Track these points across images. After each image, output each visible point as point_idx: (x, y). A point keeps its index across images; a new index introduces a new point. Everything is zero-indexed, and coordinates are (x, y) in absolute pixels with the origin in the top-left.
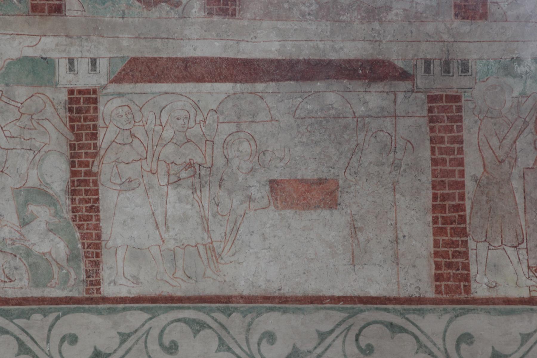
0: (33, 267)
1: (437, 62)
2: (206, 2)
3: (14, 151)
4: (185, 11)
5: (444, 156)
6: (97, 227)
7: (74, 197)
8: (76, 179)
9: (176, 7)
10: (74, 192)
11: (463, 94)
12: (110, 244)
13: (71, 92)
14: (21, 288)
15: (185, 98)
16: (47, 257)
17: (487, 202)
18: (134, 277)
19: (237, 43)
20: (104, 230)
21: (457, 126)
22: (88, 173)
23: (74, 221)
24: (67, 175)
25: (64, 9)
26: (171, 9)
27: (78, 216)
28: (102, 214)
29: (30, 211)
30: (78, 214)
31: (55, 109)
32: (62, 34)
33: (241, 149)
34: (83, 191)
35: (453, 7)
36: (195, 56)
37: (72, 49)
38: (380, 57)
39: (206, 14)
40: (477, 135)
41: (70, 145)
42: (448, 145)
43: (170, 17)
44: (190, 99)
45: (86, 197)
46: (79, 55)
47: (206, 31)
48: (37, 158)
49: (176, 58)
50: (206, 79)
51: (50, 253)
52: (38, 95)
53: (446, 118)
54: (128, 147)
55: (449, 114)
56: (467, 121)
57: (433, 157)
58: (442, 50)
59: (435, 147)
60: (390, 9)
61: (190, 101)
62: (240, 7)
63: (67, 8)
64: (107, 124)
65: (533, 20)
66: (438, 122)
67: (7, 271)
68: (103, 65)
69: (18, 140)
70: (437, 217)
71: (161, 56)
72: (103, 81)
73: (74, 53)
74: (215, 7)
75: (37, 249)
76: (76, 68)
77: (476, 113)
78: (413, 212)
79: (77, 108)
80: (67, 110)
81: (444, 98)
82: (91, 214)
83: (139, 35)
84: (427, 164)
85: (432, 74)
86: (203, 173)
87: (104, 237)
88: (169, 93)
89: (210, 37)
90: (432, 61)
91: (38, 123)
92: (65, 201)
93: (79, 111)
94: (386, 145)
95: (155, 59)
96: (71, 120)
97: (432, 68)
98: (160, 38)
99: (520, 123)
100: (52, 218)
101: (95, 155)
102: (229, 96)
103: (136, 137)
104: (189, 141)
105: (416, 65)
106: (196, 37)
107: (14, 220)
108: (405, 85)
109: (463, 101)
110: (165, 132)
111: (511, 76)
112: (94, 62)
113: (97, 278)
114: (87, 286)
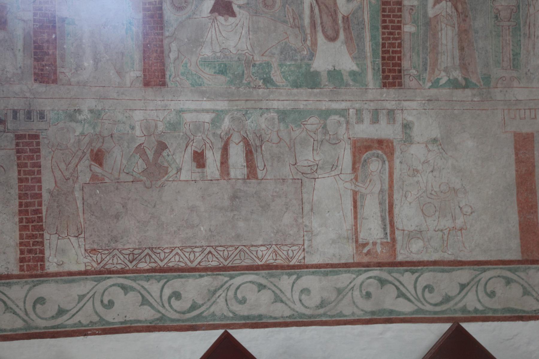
1: (22, 112)
5: (27, 176)
11: (41, 134)
17: (58, 207)
21: (37, 155)
35: (33, 75)
40: (50, 162)
42: (30, 169)
53: (28, 150)
55: (30, 148)
56: (43, 152)
57: (20, 177)
58: (25, 104)
59: (21, 170)
65: (89, 85)
66: (22, 153)
70: (22, 219)
77: (50, 146)
78: (4, 216)
81: (27, 136)
84: (14, 182)
85: (18, 120)
90: (18, 111)
97: (18, 116)
99: (80, 153)
105: (6, 114)
109: (41, 139)
111: (74, 121)
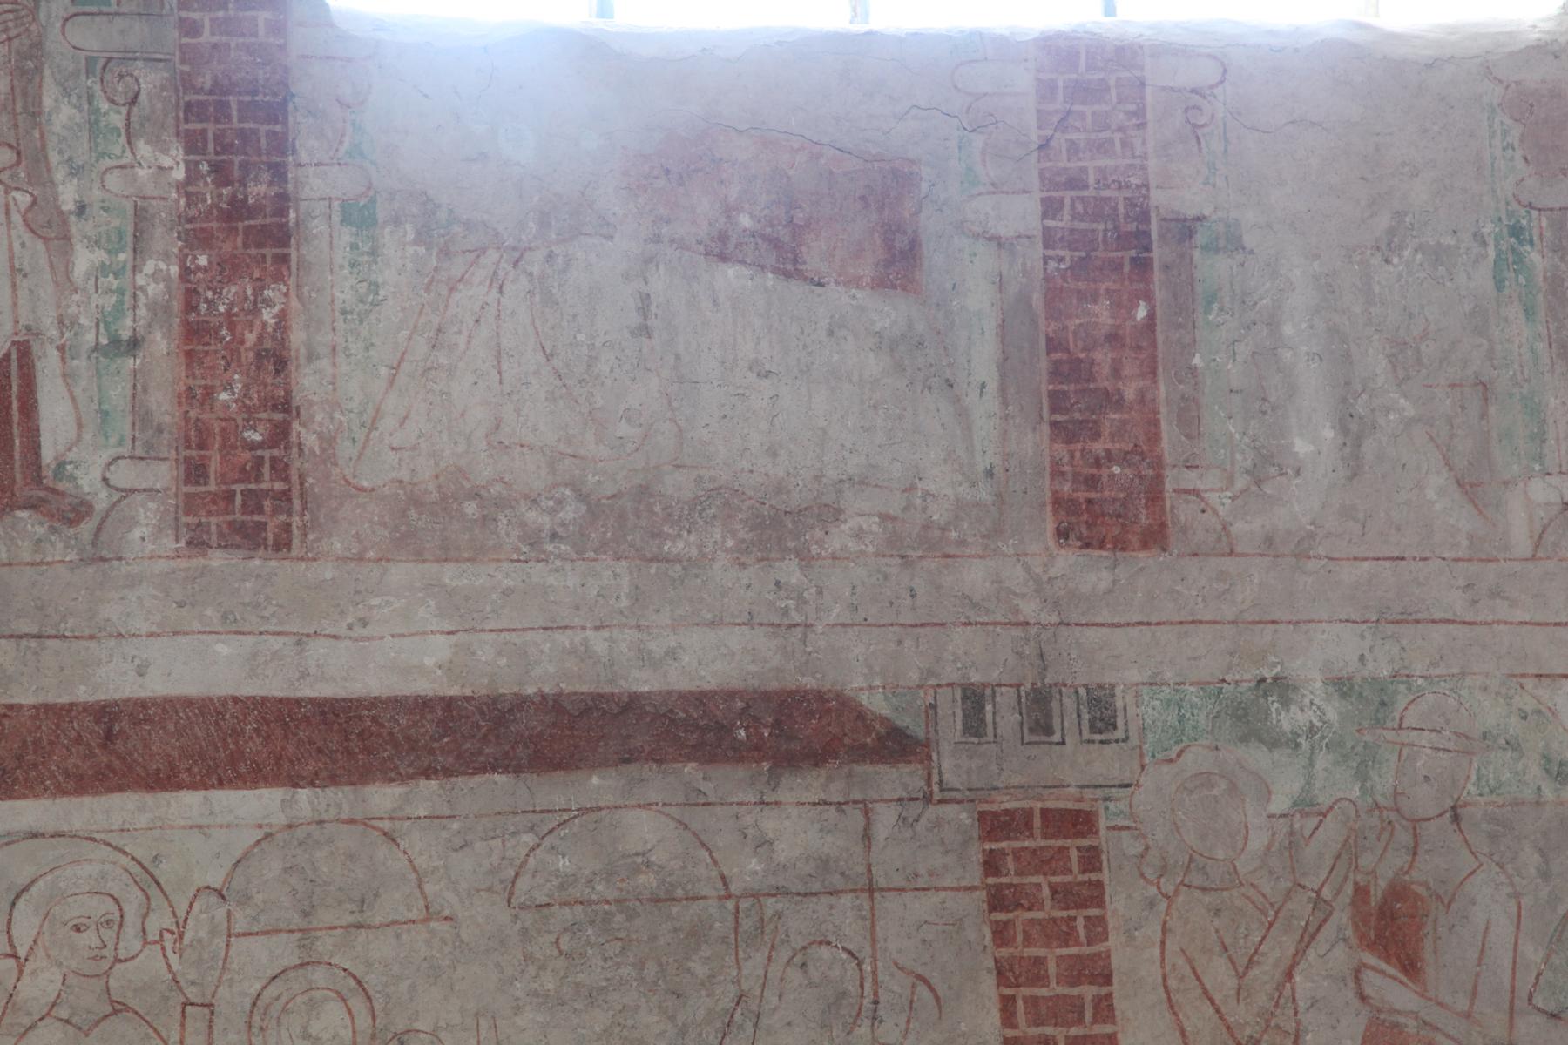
1: (1006, 697)
2: (181, 505)
4: (104, 537)
5: (1049, 1030)
9: (72, 523)
11: (1101, 805)
15: (105, 851)
19: (298, 643)
21: (1087, 918)
26: (53, 530)
33: (315, 1028)
35: (1049, 508)
36: (143, 694)
38: (809, 682)
39: (182, 544)
40: (1157, 951)
42: (1060, 990)
43: (49, 559)
44: (125, 853)
47: (181, 605)
49: (72, 704)
50: (184, 776)
53: (1046, 892)
55: (1057, 879)
56: (1119, 904)
57: (1010, 1033)
58: (1020, 655)
59: (1013, 998)
60: (837, 514)
61: (125, 860)
62: (307, 517)
65: (1321, 551)
66: (1019, 906)
71: (15, 701)
74: (213, 520)
77: (1150, 873)
81: (1037, 822)
85: (990, 738)
88: (43, 835)
89: (197, 626)
90: (988, 692)
94: (844, 994)
97: (989, 717)
98: (11, 636)
99: (1300, 906)
102: (268, 836)
104: (118, 1008)
105: (933, 707)
106: (145, 628)
108: (895, 779)
109: (1102, 832)
110: (26, 978)
111: (1261, 740)
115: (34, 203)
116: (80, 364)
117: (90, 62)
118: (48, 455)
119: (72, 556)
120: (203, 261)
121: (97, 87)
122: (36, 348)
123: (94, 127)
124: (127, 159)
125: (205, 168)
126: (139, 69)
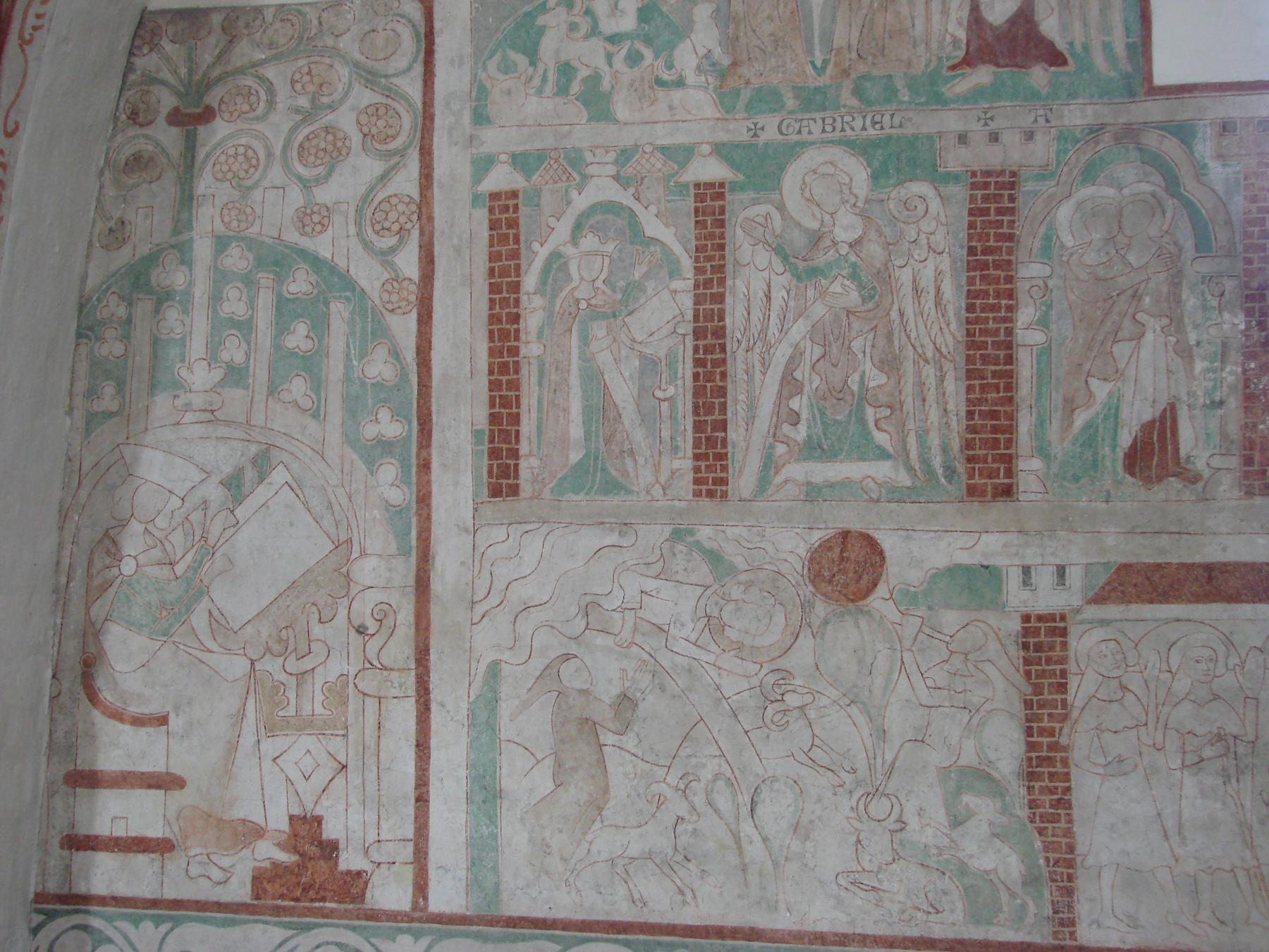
0: (970, 893)
3: (941, 709)
6: (1068, 833)
7: (1031, 784)
8: (1034, 755)
10: (1032, 776)
12: (1090, 861)
13: (1026, 618)
14: (953, 924)
15: (1208, 629)
16: (992, 877)
18: (1129, 916)
20: (1079, 839)
22: (1053, 747)
23: (1031, 822)
24: (1019, 749)
25: (1015, 490)
27: (1037, 814)
28: (1076, 813)
29: (964, 803)
30: (1038, 811)
31: (1002, 645)
32: (1013, 529)
34: (1046, 776)
37: (1028, 551)
39: (1242, 493)
41: (1026, 702)
45: (1050, 784)
46: (1039, 560)
47: (1242, 521)
48: (975, 721)
50: (1243, 597)
51: (995, 870)
52: (975, 623)
54: (1115, 706)
63: (1021, 489)
64: (1083, 669)
67: (930, 895)
68: (1075, 576)
69: (945, 692)
72: (1076, 601)
73: (1031, 557)
74: (1256, 483)
75: (975, 864)
76: (1033, 581)
79: (1035, 644)
80: (1021, 646)
82: (1059, 811)
83: (1133, 528)
86: (1241, 750)
87: (1080, 849)
91: (976, 666)
92: (1017, 790)
93: (1038, 647)
95: (1159, 565)
96: (1027, 662)
100: (998, 815)
101: (1064, 718)
103: (1129, 690)
104: (1216, 697)
107: (941, 817)
110: (1175, 682)
112: (1061, 571)
113: (1071, 915)
114: (1054, 926)
115: (1178, 341)
116: (1197, 412)
117: (1203, 277)
118: (1183, 453)
119: (1194, 498)
120: (1253, 365)
121: (1206, 290)
122: (1178, 406)
123: (1205, 308)
124: (1219, 320)
125: (1254, 323)
126: (1225, 280)
